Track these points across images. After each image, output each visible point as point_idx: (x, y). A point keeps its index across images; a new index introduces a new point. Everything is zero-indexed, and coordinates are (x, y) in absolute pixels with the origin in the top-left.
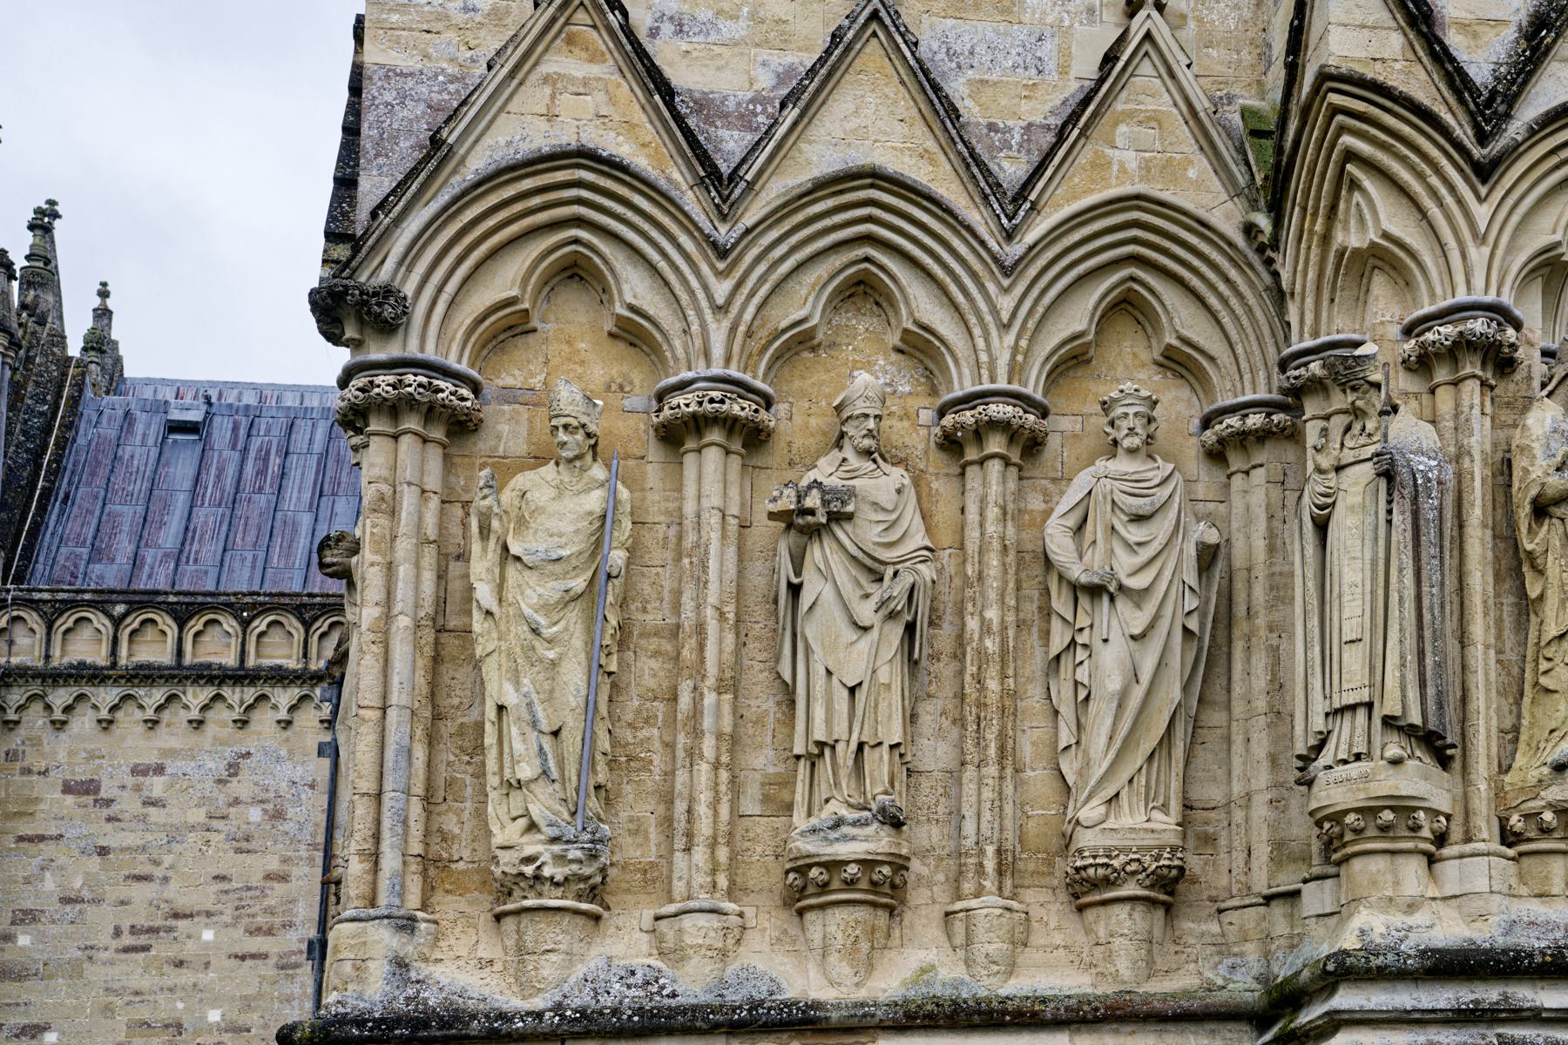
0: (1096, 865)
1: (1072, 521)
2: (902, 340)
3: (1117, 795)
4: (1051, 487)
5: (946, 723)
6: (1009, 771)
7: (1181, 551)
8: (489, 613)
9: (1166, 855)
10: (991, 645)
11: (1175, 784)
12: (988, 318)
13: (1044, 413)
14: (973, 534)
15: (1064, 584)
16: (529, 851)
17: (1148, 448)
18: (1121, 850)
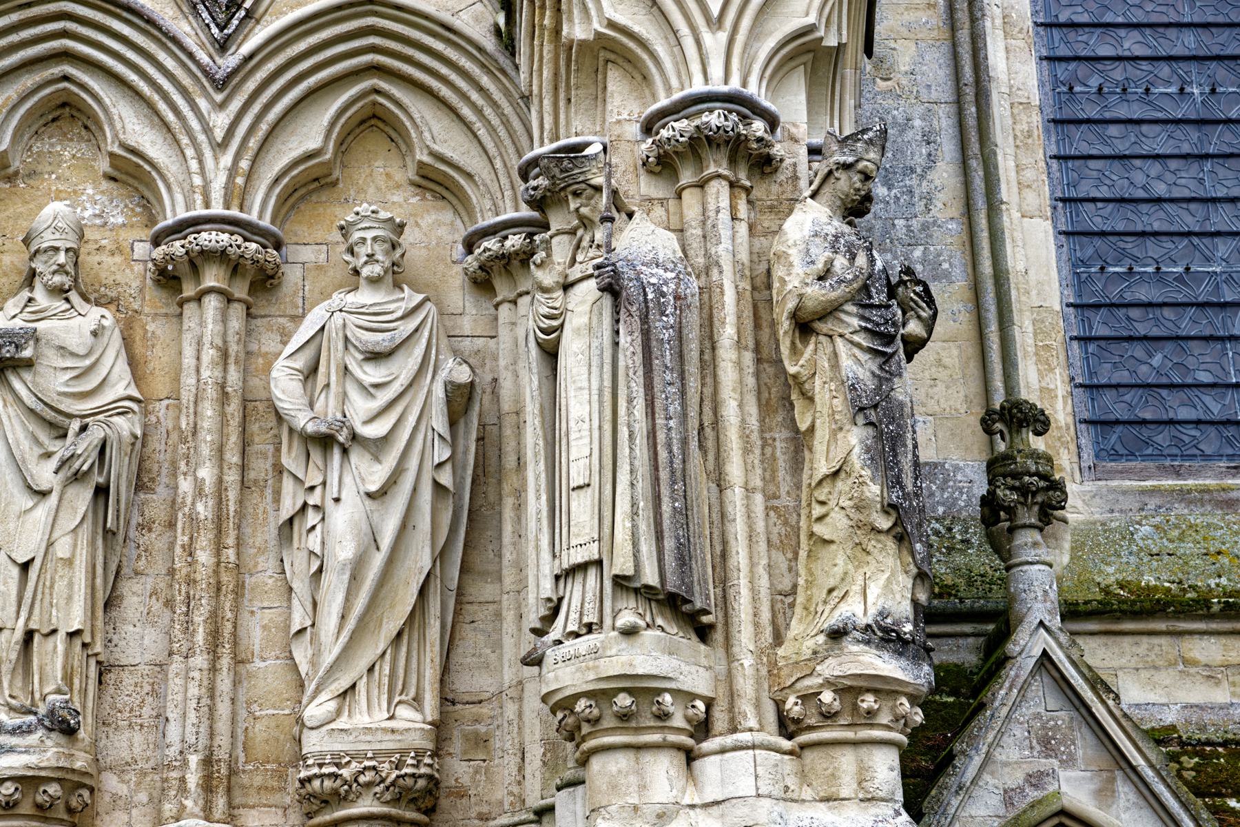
0: (322, 776)
1: (300, 362)
2: (112, 165)
3: (353, 686)
5: (157, 606)
6: (225, 662)
7: (429, 392)
9: (410, 761)
10: (204, 510)
11: (431, 674)
12: (202, 138)
13: (278, 246)
14: (189, 381)
17: (395, 276)
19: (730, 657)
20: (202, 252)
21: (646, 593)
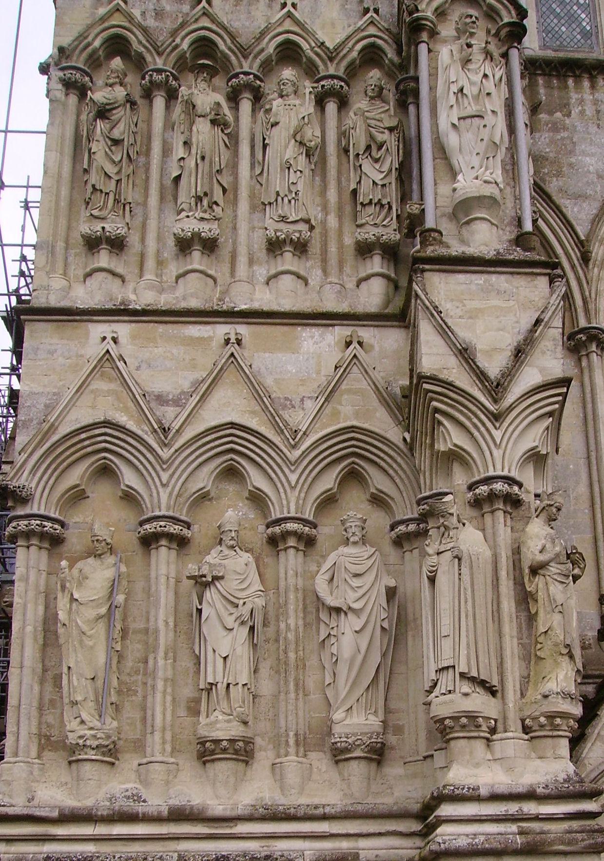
0: (341, 742)
1: (327, 576)
4: (321, 560)
5: (273, 673)
7: (378, 590)
8: (64, 625)
10: (291, 636)
11: (381, 703)
12: (286, 484)
14: (282, 584)
15: (325, 607)
16: (82, 733)
17: (364, 541)
18: (354, 734)
19: (504, 703)
20: (287, 531)
21: (473, 680)
